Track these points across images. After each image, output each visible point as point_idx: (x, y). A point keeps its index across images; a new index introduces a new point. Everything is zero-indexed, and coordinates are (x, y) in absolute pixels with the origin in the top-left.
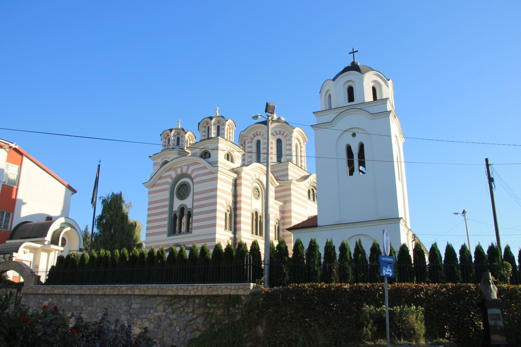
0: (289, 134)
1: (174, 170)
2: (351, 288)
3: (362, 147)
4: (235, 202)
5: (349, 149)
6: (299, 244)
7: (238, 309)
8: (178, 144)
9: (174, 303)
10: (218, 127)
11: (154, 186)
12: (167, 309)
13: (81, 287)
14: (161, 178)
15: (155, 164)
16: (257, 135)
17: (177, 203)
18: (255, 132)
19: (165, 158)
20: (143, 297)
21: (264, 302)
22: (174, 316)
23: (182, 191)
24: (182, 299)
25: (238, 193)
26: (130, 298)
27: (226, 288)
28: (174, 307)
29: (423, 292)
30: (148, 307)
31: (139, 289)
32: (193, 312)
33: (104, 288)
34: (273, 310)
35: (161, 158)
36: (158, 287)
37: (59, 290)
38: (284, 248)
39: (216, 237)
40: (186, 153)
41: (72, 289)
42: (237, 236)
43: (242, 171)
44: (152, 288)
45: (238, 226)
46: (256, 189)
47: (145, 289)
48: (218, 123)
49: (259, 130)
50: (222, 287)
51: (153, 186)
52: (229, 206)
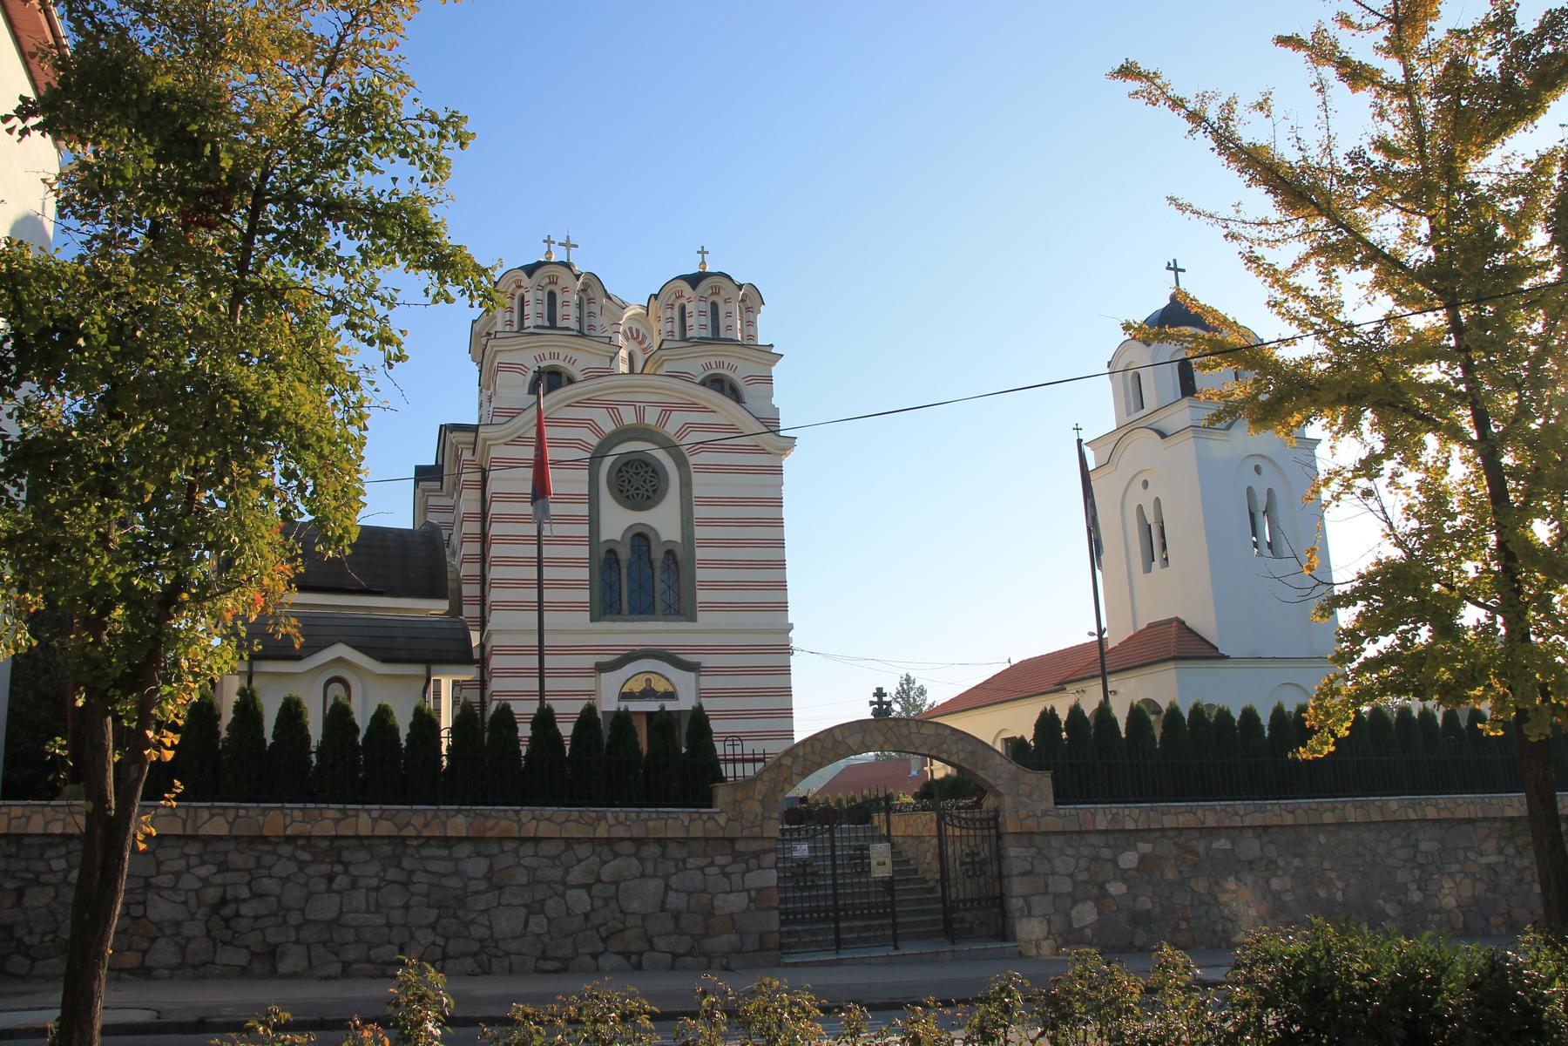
13: (1261, 805)
17: (617, 521)
19: (553, 356)
31: (1436, 806)
35: (537, 352)
37: (1181, 818)
41: (1227, 812)
51: (512, 443)
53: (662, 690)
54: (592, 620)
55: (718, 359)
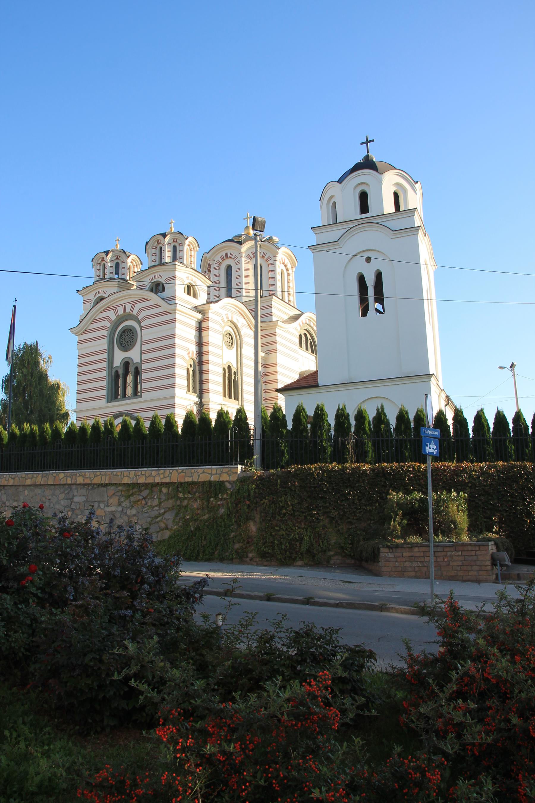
0: (271, 256)
2: (372, 470)
3: (379, 276)
4: (200, 353)
5: (361, 279)
6: (302, 412)
7: (221, 499)
8: (117, 273)
9: (132, 494)
10: (175, 248)
11: (85, 332)
12: (122, 502)
14: (94, 321)
15: (85, 302)
16: (227, 258)
17: (119, 356)
18: (223, 253)
19: (99, 292)
20: (88, 486)
21: (256, 490)
22: (134, 512)
24: (143, 488)
25: (204, 340)
26: (71, 489)
27: (204, 472)
28: (132, 499)
29: (466, 473)
30: (96, 500)
31: (83, 476)
32: (159, 505)
33: (33, 477)
34: (270, 501)
35: (94, 293)
36: (109, 473)
38: (281, 418)
39: (176, 402)
40: (128, 285)
42: (203, 400)
43: (209, 309)
44: (101, 474)
45: (205, 386)
46: (228, 334)
47: (91, 476)
48: (174, 242)
49: (229, 252)
50: (199, 471)
52: (192, 359)
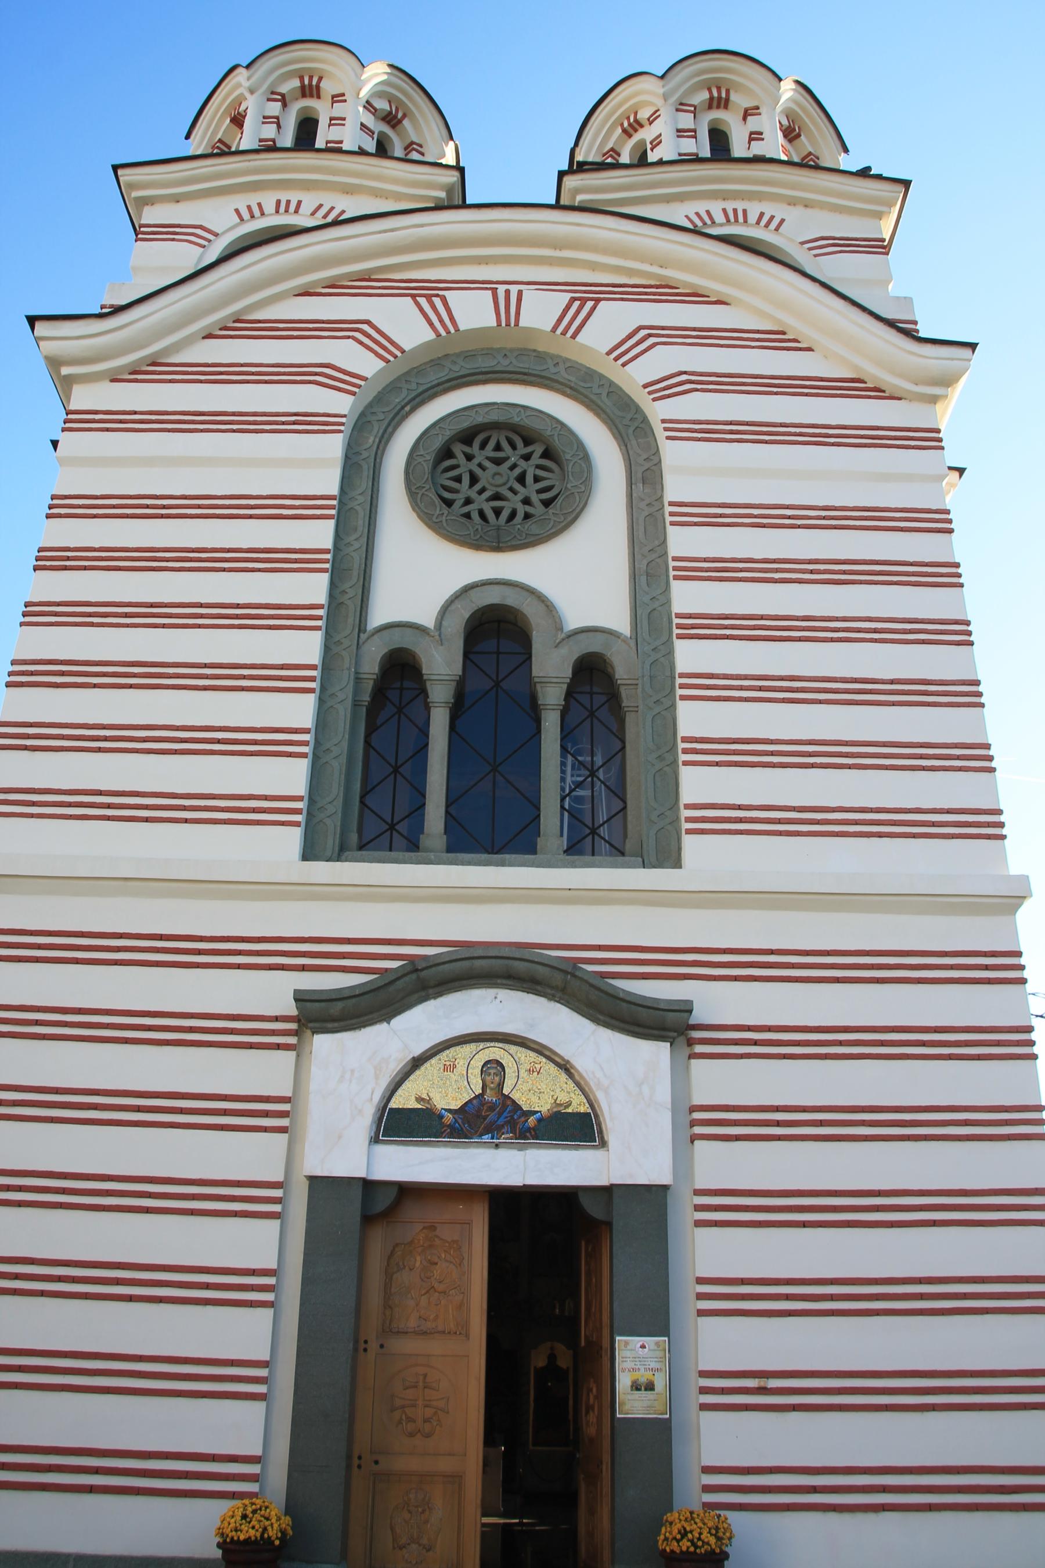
1: (414, 297)
23: (474, 480)
35: (241, 201)
51: (135, 374)
53: (543, 1105)
54: (308, 854)
55: (730, 206)
